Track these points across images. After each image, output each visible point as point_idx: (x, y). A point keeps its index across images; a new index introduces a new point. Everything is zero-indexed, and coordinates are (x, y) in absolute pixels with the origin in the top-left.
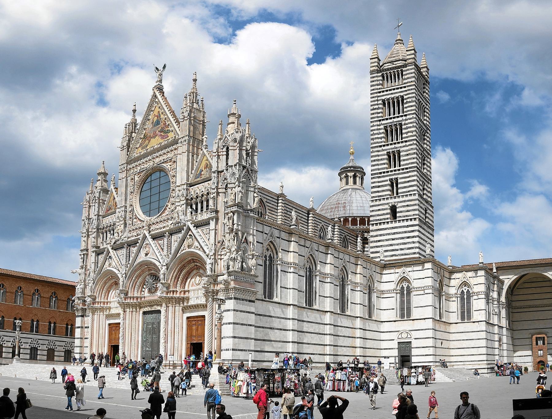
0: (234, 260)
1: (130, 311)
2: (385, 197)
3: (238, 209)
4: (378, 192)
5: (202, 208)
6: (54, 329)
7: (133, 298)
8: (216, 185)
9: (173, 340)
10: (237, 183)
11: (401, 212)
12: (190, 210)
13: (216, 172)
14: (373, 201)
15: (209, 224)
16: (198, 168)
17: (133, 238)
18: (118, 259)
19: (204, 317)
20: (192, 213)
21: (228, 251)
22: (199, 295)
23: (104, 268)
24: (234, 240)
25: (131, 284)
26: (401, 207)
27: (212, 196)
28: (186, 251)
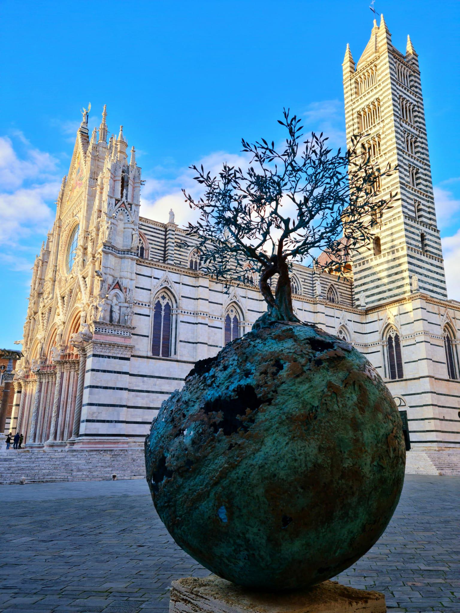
3: (105, 249)
11: (385, 243)
26: (385, 237)
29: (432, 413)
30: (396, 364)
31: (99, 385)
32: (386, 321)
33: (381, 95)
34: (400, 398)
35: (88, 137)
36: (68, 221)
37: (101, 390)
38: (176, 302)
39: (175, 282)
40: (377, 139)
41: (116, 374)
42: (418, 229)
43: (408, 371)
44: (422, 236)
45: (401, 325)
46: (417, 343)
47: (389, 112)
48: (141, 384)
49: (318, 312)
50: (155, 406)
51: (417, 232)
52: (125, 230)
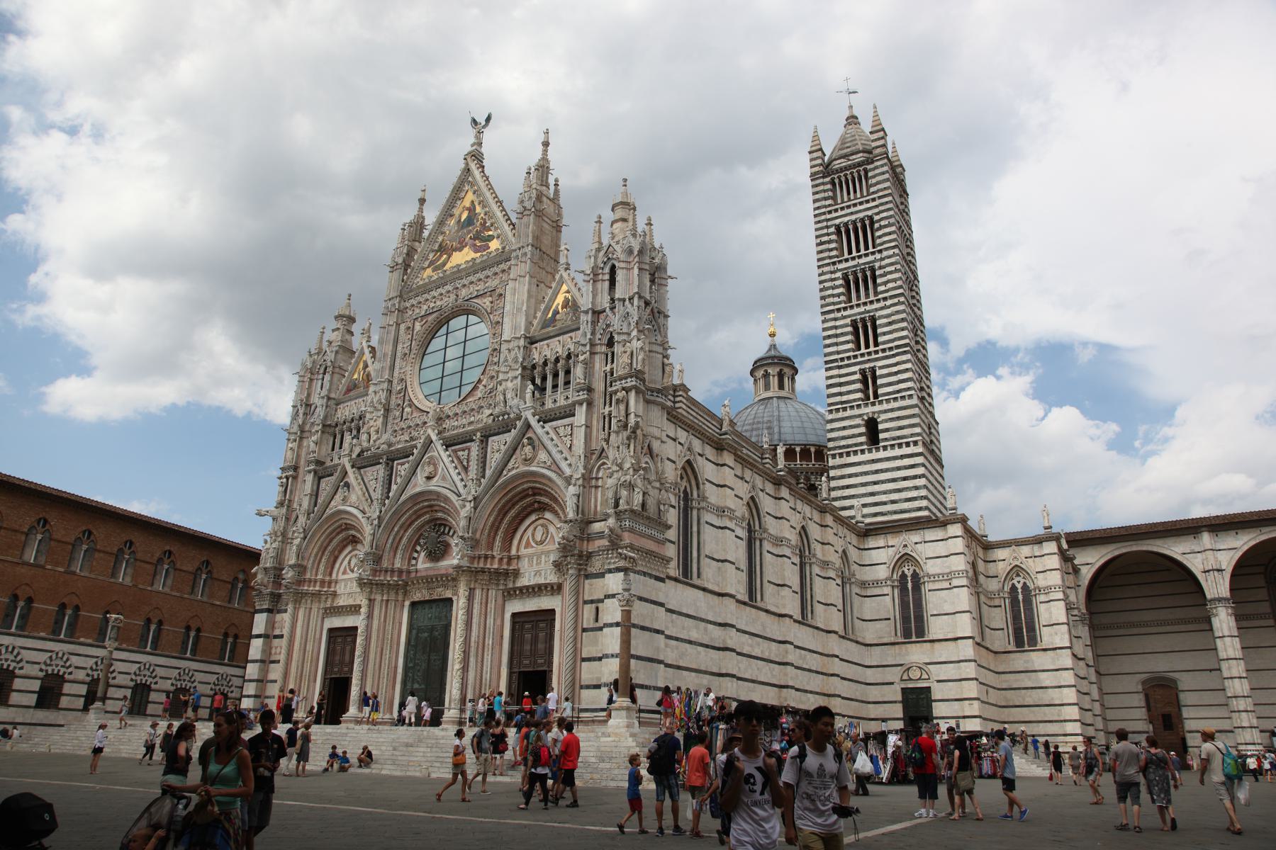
0: (631, 487)
1: (382, 600)
2: (854, 404)
4: (841, 394)
5: (555, 386)
6: (195, 644)
7: (393, 571)
8: (589, 336)
9: (479, 665)
10: (634, 333)
11: (887, 430)
12: (531, 387)
13: (590, 312)
14: (831, 412)
15: (574, 415)
16: (548, 309)
18: (364, 488)
19: (552, 612)
22: (543, 565)
23: (330, 506)
24: (629, 445)
25: (390, 541)
27: (581, 358)
28: (518, 470)
29: (976, 691)
30: (912, 616)
32: (901, 549)
33: (877, 214)
34: (920, 668)
35: (483, 167)
36: (432, 305)
38: (698, 488)
39: (699, 454)
40: (868, 273)
43: (936, 628)
45: (926, 559)
46: (955, 587)
48: (670, 625)
49: (827, 526)
50: (684, 665)
51: (926, 421)
52: (651, 354)
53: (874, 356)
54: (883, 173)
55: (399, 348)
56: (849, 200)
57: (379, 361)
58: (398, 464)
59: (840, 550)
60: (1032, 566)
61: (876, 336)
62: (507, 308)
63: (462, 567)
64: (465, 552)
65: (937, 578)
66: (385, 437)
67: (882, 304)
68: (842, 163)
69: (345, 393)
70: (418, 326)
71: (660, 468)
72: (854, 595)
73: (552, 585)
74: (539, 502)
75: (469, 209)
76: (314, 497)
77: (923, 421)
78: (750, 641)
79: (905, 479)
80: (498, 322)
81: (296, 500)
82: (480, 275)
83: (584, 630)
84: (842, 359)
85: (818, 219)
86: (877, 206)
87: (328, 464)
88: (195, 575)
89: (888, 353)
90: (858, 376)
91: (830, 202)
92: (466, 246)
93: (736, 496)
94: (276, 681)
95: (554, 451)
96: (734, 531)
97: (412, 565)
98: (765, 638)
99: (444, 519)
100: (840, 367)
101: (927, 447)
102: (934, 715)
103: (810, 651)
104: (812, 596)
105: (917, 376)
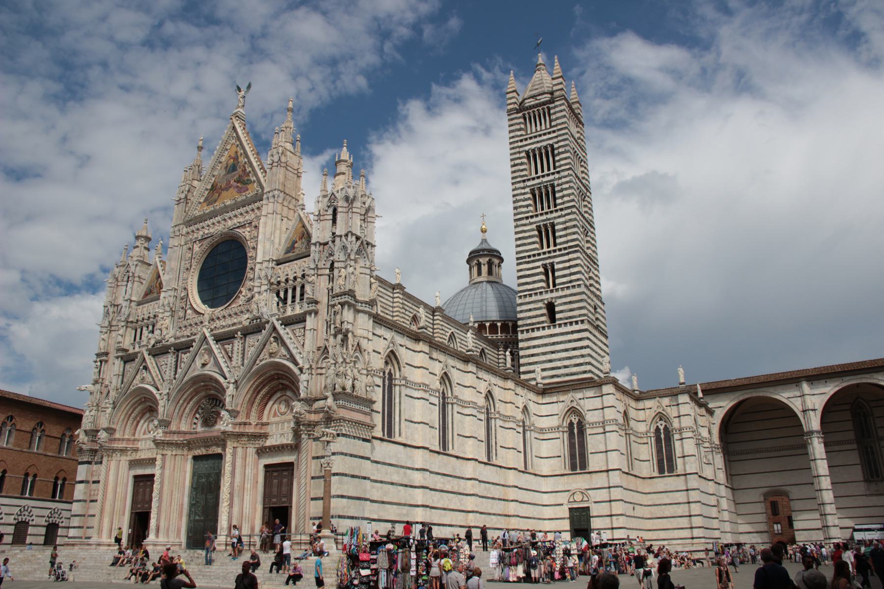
3: (349, 300)
5: (294, 297)
11: (561, 312)
12: (276, 299)
13: (318, 244)
14: (520, 297)
15: (305, 321)
17: (183, 340)
18: (158, 372)
20: (278, 305)
21: (333, 362)
22: (286, 430)
23: (133, 384)
25: (177, 411)
26: (561, 304)
31: (347, 472)
36: (206, 232)
37: (349, 478)
38: (400, 370)
39: (401, 345)
40: (550, 189)
41: (361, 460)
42: (592, 300)
43: (595, 462)
44: (595, 309)
47: (566, 164)
50: (387, 500)
51: (592, 303)
53: (553, 254)
54: (561, 111)
55: (183, 264)
56: (537, 131)
57: (168, 274)
58: (182, 353)
59: (521, 406)
60: (672, 412)
61: (555, 238)
62: (260, 237)
63: (226, 432)
64: (230, 421)
65: (598, 425)
66: (172, 332)
67: (559, 213)
68: (532, 102)
69: (143, 298)
70: (196, 248)
71: (367, 360)
72: (533, 438)
73: (291, 446)
74: (282, 384)
75: (234, 159)
76: (121, 377)
77: (589, 304)
78: (442, 480)
79: (574, 349)
80: (254, 248)
81: (108, 377)
82: (242, 210)
83: (313, 478)
84: (529, 256)
85: (512, 146)
86: (556, 137)
87: (131, 351)
88: (32, 434)
89: (563, 252)
90: (541, 270)
91: (523, 132)
92: (231, 187)
93: (430, 373)
94: (94, 516)
95: (291, 347)
96: (428, 400)
97: (194, 429)
98: (455, 477)
99: (215, 395)
100: (528, 262)
101: (592, 324)
102: (592, 528)
103: (493, 484)
104: (496, 443)
105: (586, 268)
